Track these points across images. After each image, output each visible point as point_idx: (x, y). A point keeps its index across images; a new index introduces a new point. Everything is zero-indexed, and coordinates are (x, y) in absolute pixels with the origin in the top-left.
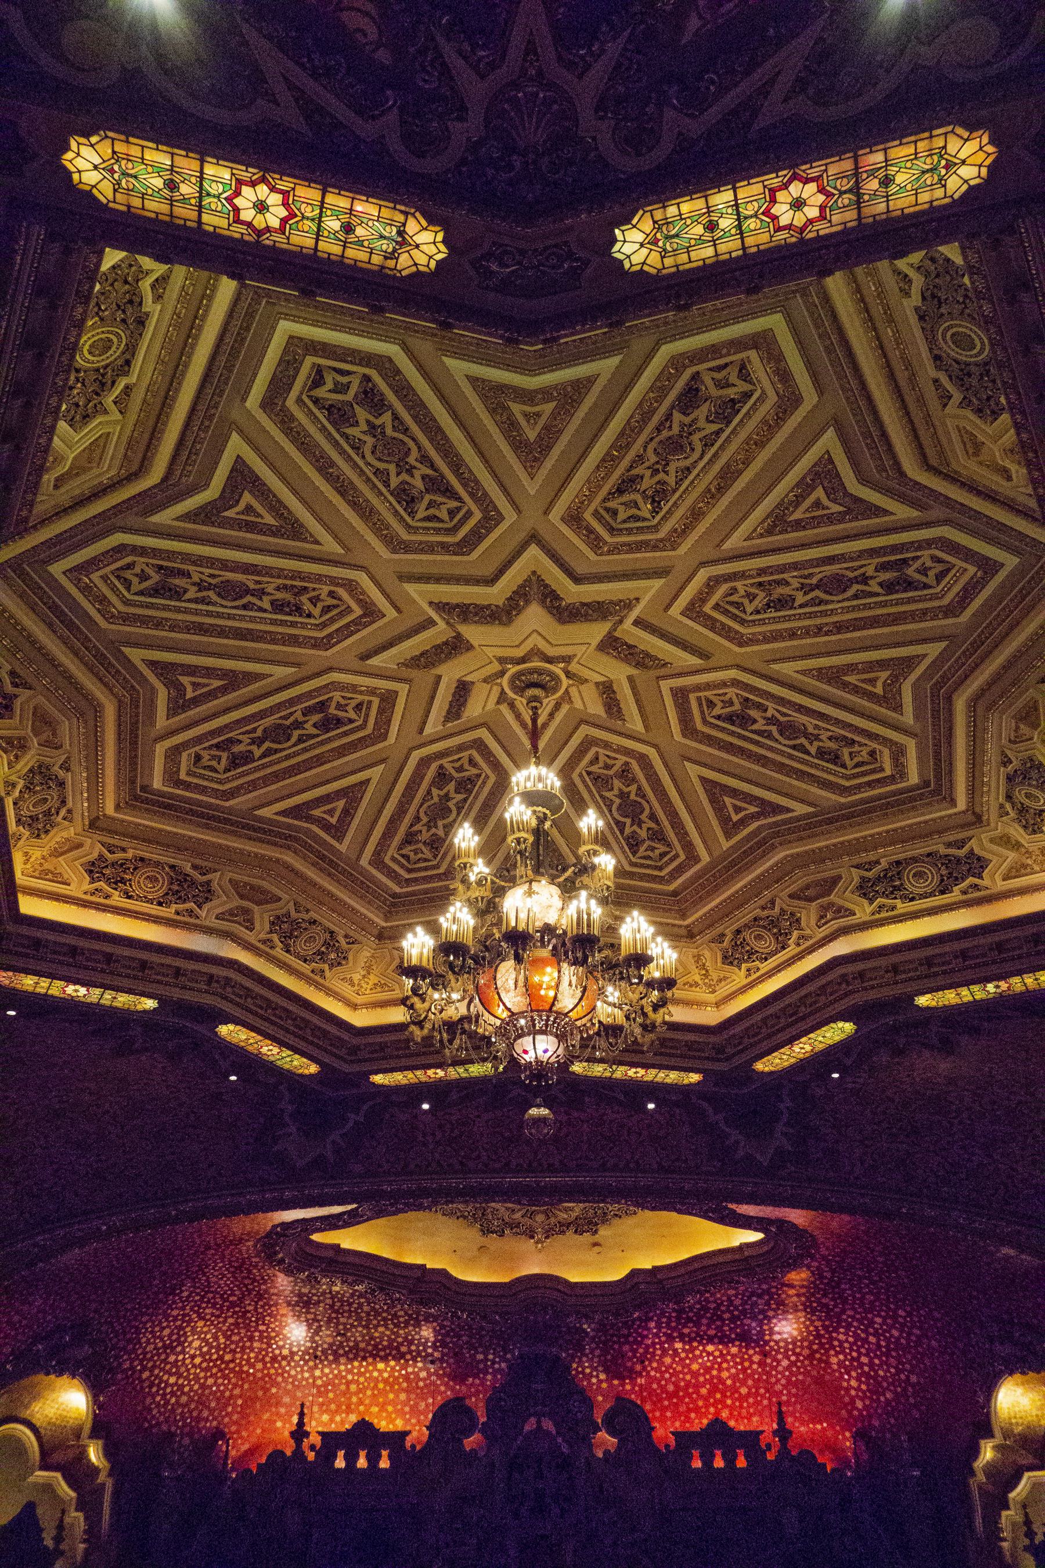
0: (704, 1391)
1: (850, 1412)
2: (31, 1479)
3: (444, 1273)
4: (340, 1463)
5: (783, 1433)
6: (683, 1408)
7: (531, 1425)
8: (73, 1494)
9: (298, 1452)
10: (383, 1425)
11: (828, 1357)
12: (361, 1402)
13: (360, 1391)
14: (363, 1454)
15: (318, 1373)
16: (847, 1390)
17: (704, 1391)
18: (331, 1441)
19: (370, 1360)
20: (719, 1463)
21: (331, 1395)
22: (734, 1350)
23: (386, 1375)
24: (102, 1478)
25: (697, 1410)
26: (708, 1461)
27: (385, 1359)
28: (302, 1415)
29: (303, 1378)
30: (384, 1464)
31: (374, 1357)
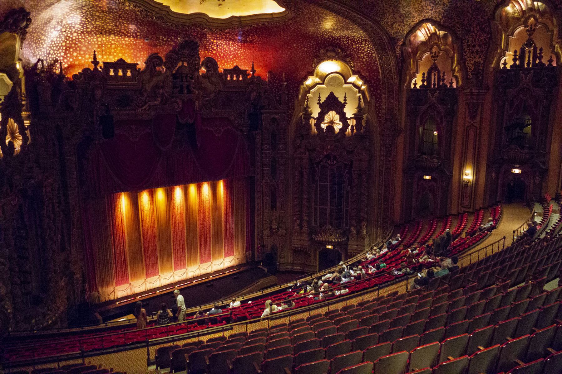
0: (231, 57)
3: (168, 7)
4: (112, 73)
5: (253, 71)
6: (223, 62)
7: (180, 64)
9: (96, 69)
10: (129, 61)
12: (115, 52)
13: (115, 47)
14: (120, 71)
15: (100, 39)
17: (231, 57)
18: (108, 65)
19: (123, 36)
21: (103, 48)
23: (127, 43)
25: (227, 62)
26: (232, 78)
27: (129, 37)
29: (93, 41)
30: (129, 74)
31: (125, 35)
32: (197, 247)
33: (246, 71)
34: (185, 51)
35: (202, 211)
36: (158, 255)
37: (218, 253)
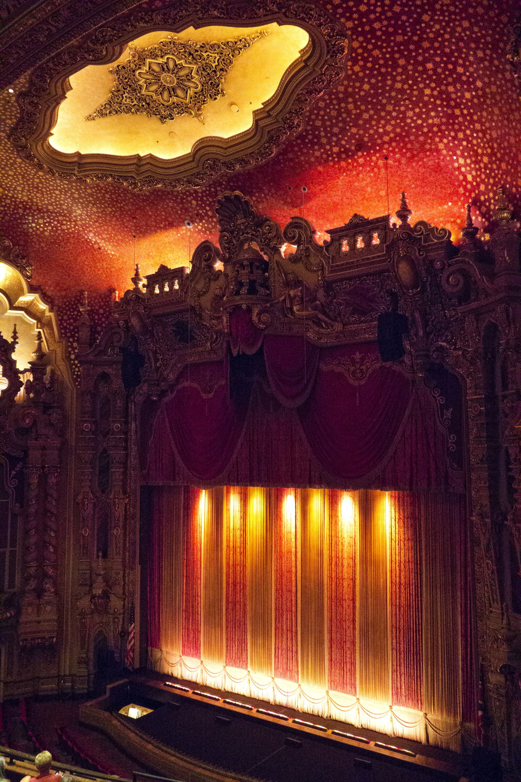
1: (465, 188)
2: (6, 314)
3: (151, 157)
4: (157, 291)
8: (35, 321)
9: (137, 289)
11: (436, 145)
14: (166, 285)
16: (459, 168)
20: (360, 244)
22: (361, 160)
24: (48, 314)
28: (137, 270)
30: (177, 287)
32: (322, 644)
33: (386, 219)
34: (239, 222)
35: (336, 560)
36: (249, 627)
37: (374, 681)
